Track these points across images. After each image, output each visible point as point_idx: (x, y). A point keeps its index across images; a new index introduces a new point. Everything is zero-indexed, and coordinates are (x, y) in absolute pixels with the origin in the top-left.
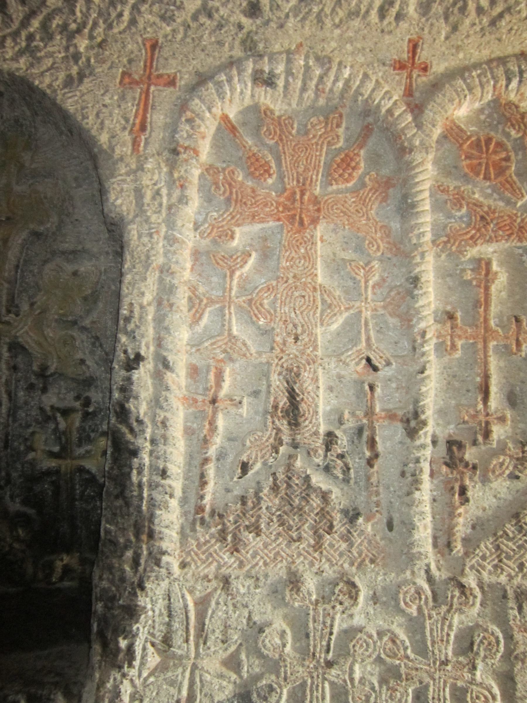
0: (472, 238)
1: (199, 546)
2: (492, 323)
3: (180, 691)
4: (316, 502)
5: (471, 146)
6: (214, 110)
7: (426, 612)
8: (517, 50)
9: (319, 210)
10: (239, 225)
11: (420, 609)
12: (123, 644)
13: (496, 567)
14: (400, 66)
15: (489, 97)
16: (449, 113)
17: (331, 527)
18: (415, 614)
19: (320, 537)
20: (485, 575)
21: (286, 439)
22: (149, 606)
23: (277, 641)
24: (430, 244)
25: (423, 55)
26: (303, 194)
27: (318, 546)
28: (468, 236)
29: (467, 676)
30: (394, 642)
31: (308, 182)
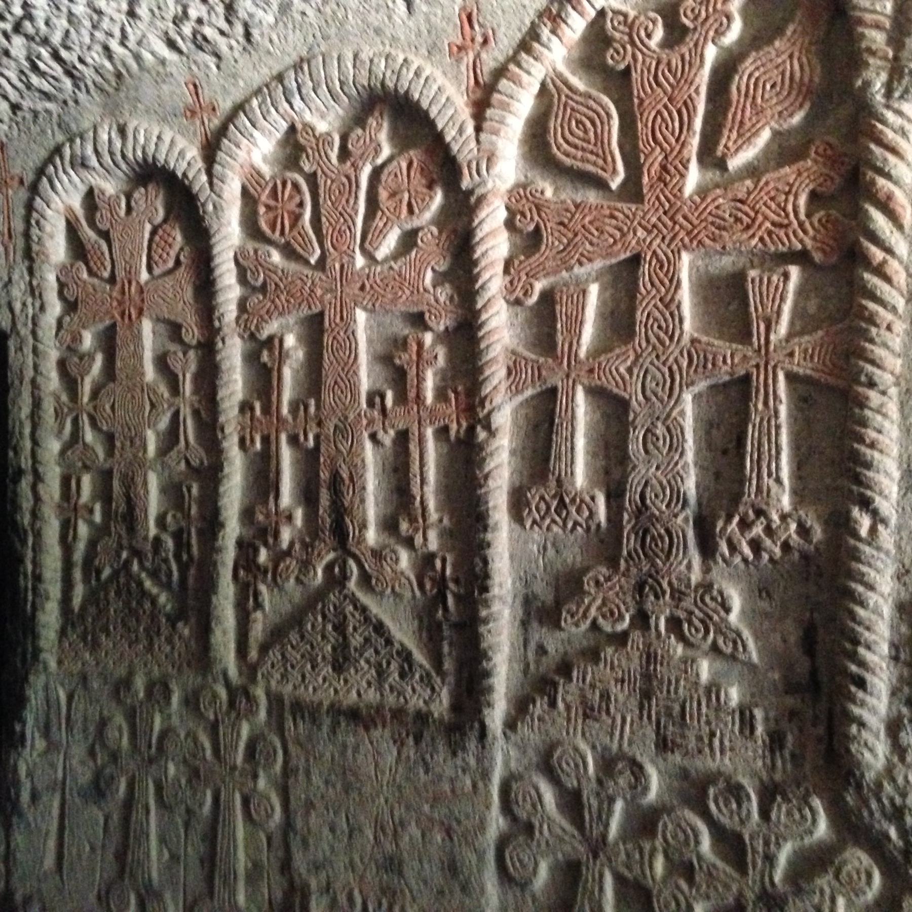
0: (268, 312)
1: (70, 645)
2: (285, 410)
3: (56, 772)
4: (147, 605)
5: (268, 197)
6: (53, 206)
7: (220, 717)
8: (295, 57)
9: (143, 301)
10: (84, 327)
11: (216, 714)
12: (18, 728)
13: (282, 676)
14: (192, 113)
15: (284, 126)
16: (240, 160)
17: (159, 630)
18: (212, 717)
19: (152, 640)
20: (273, 683)
21: (125, 542)
22: (33, 696)
23: (117, 734)
24: (234, 325)
25: (206, 94)
26: (130, 283)
27: (150, 648)
28: (265, 310)
29: (251, 784)
30: (195, 744)
31: (133, 270)
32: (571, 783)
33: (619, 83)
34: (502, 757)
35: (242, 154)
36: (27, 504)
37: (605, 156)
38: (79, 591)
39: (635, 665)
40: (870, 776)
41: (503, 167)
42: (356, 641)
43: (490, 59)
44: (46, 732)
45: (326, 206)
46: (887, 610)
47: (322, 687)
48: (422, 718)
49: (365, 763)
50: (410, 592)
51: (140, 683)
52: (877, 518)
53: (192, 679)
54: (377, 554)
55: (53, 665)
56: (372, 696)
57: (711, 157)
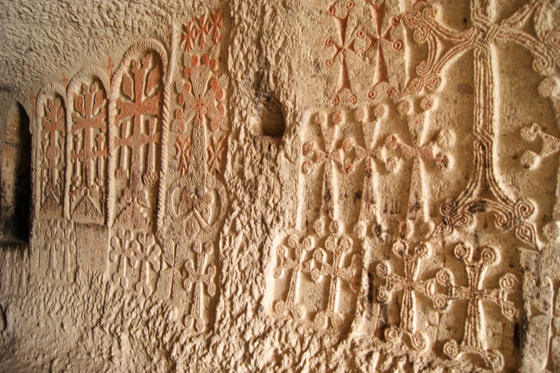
14: (64, 81)
25: (66, 76)
32: (120, 238)
33: (133, 75)
34: (111, 233)
35: (72, 90)
36: (34, 177)
37: (130, 92)
38: (44, 199)
39: (131, 210)
40: (159, 229)
41: (115, 94)
42: (88, 208)
43: (114, 69)
44: (37, 234)
45: (86, 102)
46: (164, 193)
47: (83, 220)
48: (98, 225)
49: (89, 236)
50: (99, 197)
51: (52, 221)
52: (164, 174)
53: (62, 219)
54: (92, 187)
55: (38, 217)
56: (91, 221)
57: (146, 94)
